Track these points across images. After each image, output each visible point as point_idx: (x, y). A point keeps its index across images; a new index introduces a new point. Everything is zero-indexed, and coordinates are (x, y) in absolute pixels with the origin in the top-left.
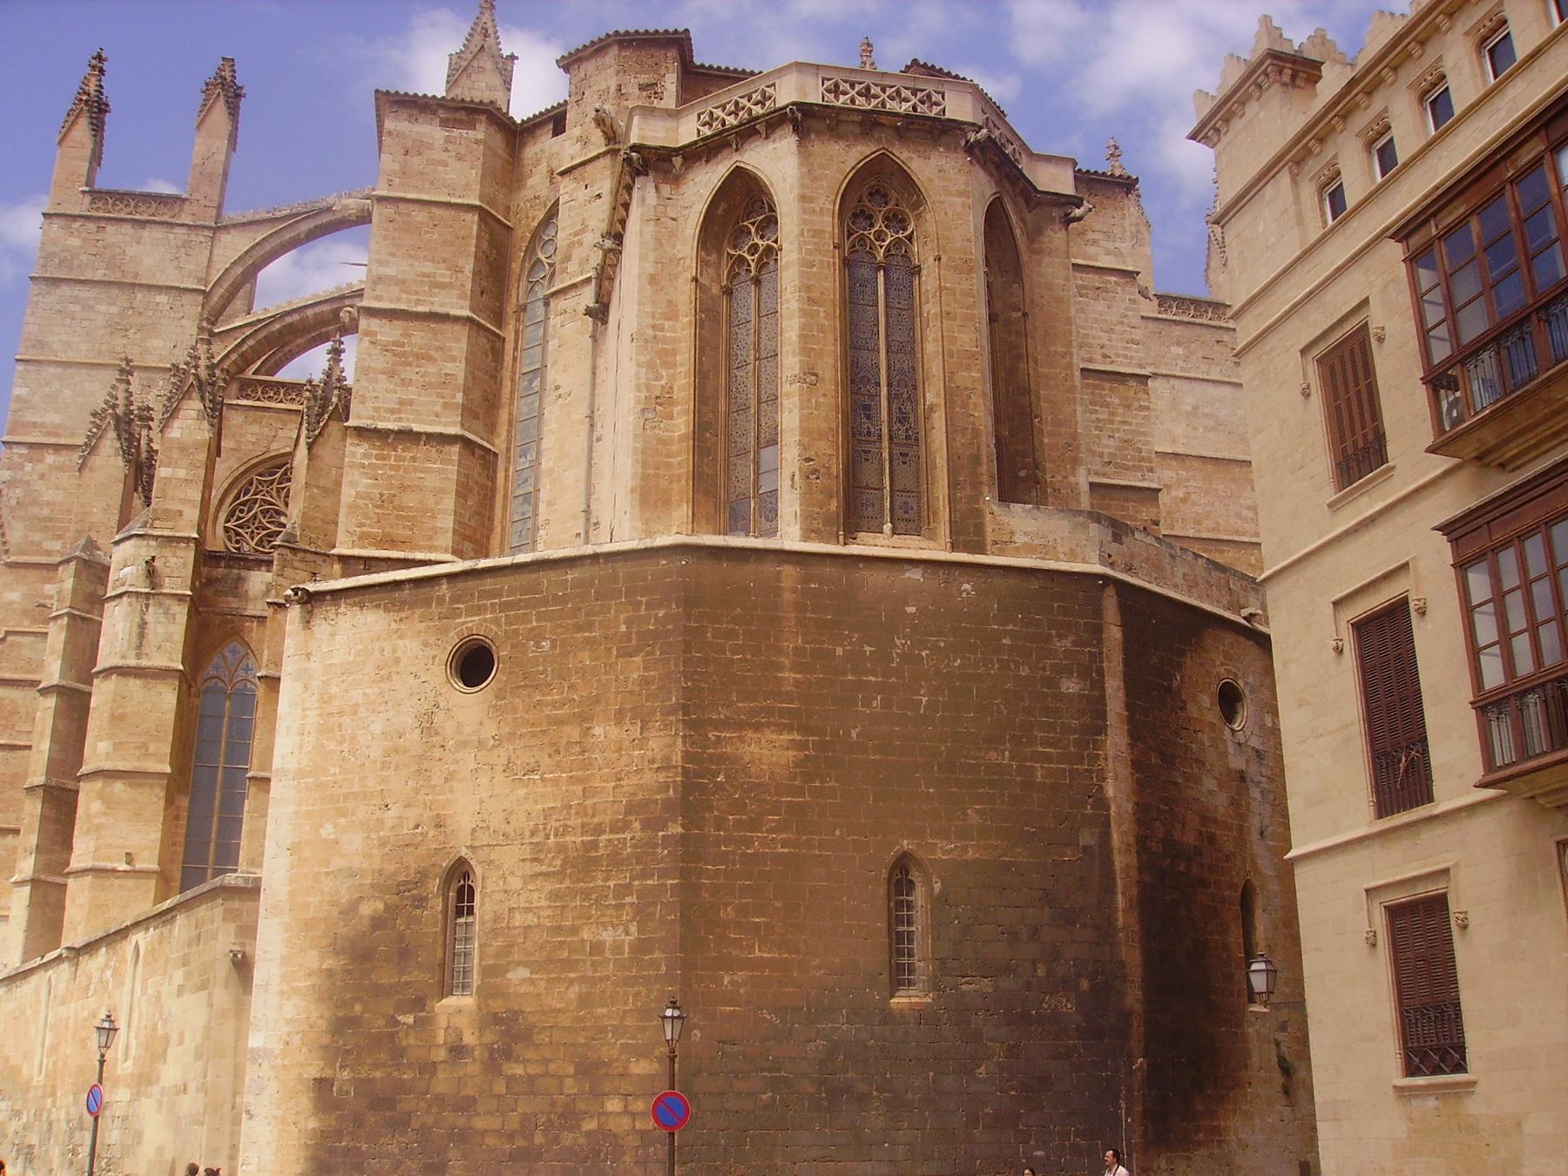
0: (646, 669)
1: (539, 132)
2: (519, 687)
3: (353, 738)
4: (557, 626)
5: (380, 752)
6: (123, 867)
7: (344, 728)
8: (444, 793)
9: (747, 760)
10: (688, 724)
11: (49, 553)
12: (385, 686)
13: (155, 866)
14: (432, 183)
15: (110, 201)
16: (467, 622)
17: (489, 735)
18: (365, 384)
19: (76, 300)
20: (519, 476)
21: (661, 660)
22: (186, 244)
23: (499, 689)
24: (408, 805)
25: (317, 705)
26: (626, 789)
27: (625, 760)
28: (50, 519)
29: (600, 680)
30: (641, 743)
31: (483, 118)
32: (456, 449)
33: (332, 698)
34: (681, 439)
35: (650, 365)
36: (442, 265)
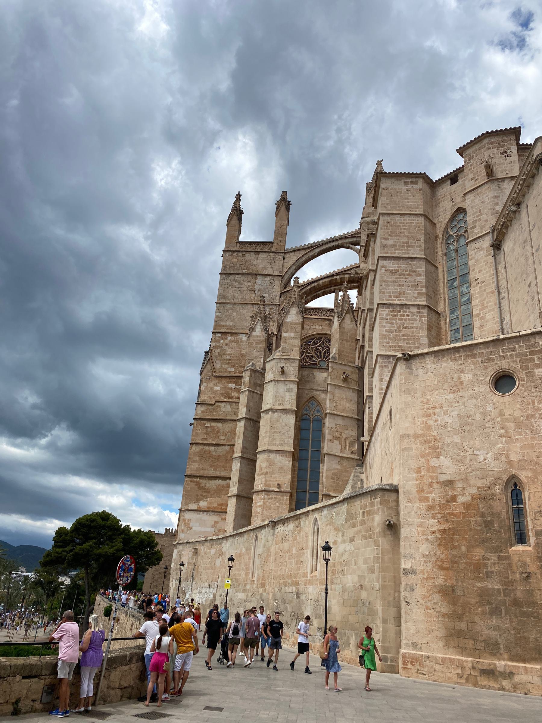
6: (277, 490)
11: (230, 372)
13: (288, 489)
15: (246, 245)
19: (236, 281)
20: (451, 322)
22: (274, 259)
28: (230, 360)
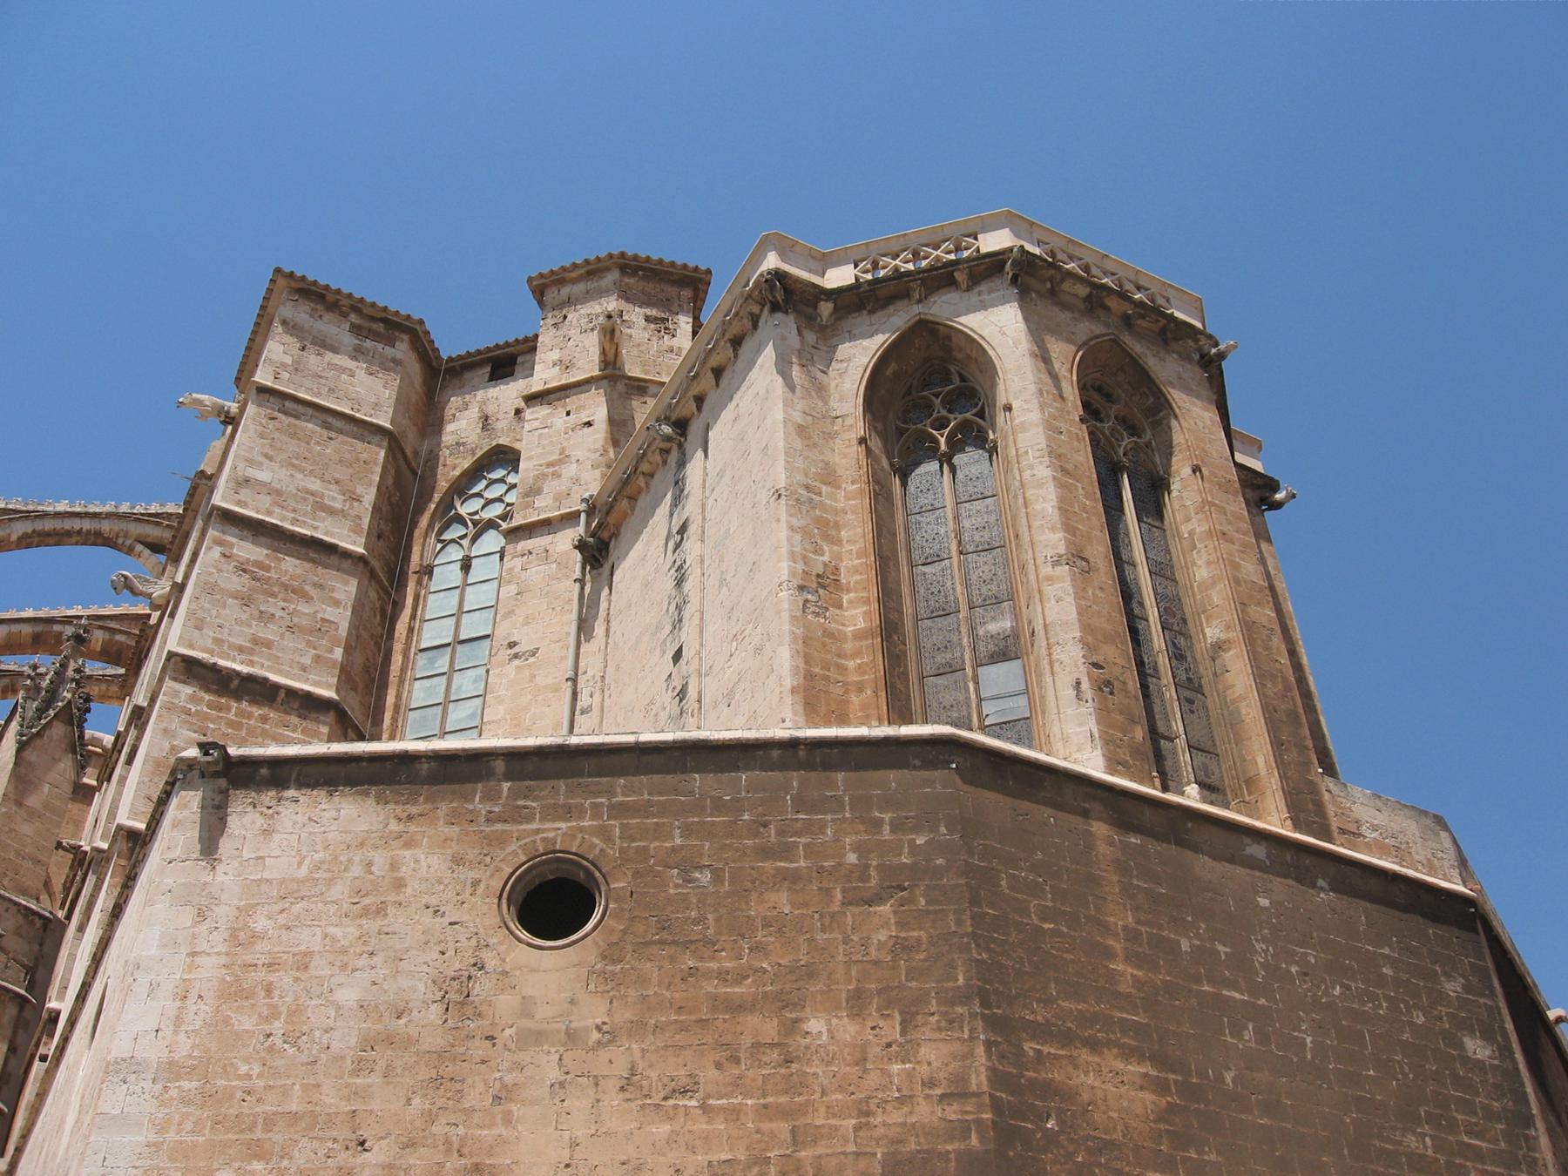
0: (901, 925)
1: (468, 375)
2: (648, 944)
3: (295, 1012)
4: (724, 847)
5: (353, 1041)
7: (277, 993)
8: (492, 1125)
9: (1085, 1097)
10: (993, 1023)
12: (371, 925)
14: (331, 390)
16: (544, 831)
17: (590, 1023)
18: (207, 606)
21: (928, 912)
23: (611, 945)
24: (411, 1144)
25: (222, 948)
26: (881, 1131)
27: (873, 1080)
29: (811, 940)
30: (907, 1052)
31: (406, 337)
32: (331, 717)
33: (255, 937)
34: (858, 636)
35: (805, 532)
36: (333, 487)
